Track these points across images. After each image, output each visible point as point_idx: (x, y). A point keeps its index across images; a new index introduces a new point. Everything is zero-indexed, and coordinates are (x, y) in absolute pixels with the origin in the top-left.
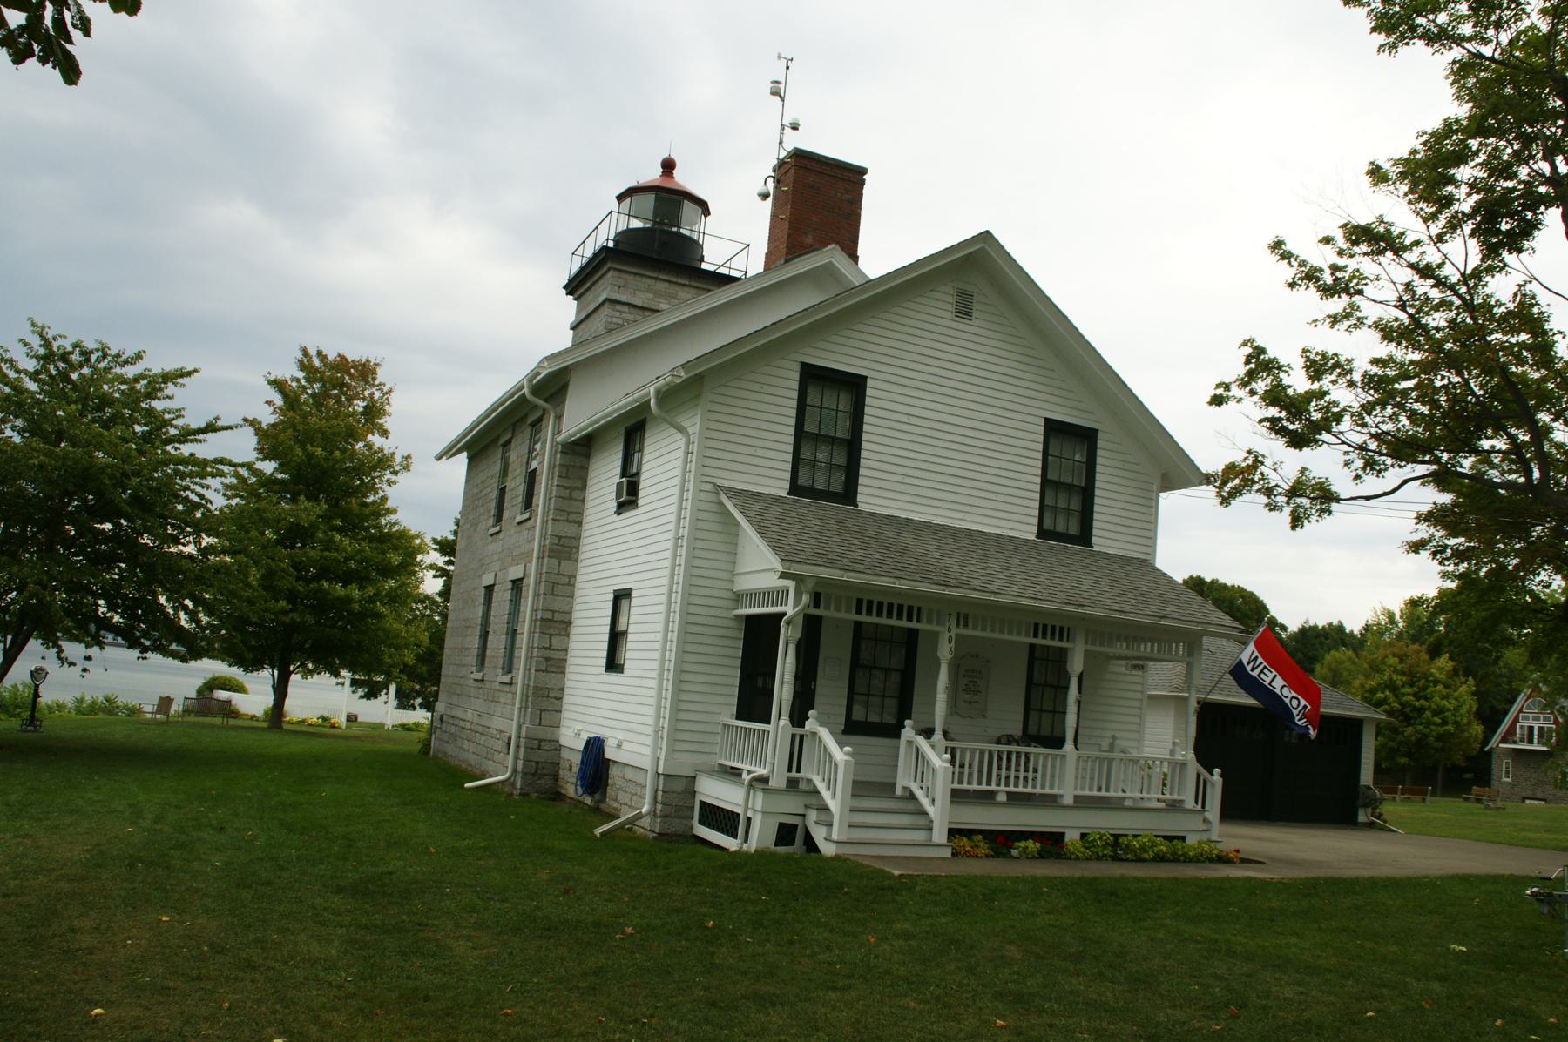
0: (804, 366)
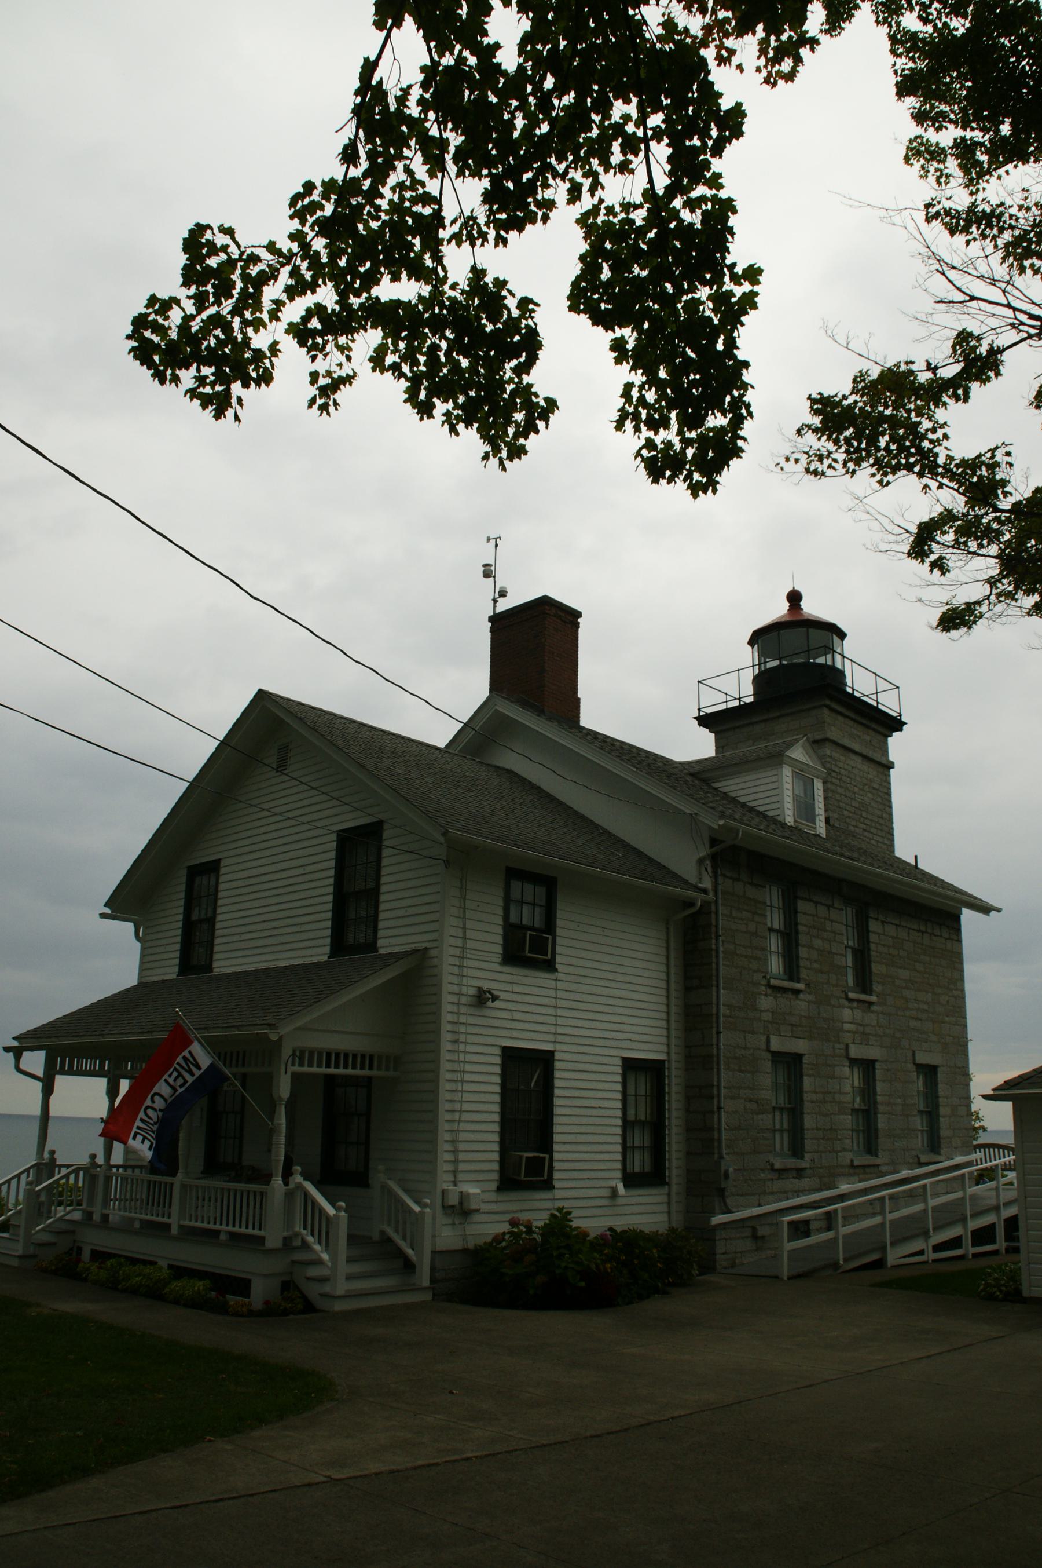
0: (189, 868)
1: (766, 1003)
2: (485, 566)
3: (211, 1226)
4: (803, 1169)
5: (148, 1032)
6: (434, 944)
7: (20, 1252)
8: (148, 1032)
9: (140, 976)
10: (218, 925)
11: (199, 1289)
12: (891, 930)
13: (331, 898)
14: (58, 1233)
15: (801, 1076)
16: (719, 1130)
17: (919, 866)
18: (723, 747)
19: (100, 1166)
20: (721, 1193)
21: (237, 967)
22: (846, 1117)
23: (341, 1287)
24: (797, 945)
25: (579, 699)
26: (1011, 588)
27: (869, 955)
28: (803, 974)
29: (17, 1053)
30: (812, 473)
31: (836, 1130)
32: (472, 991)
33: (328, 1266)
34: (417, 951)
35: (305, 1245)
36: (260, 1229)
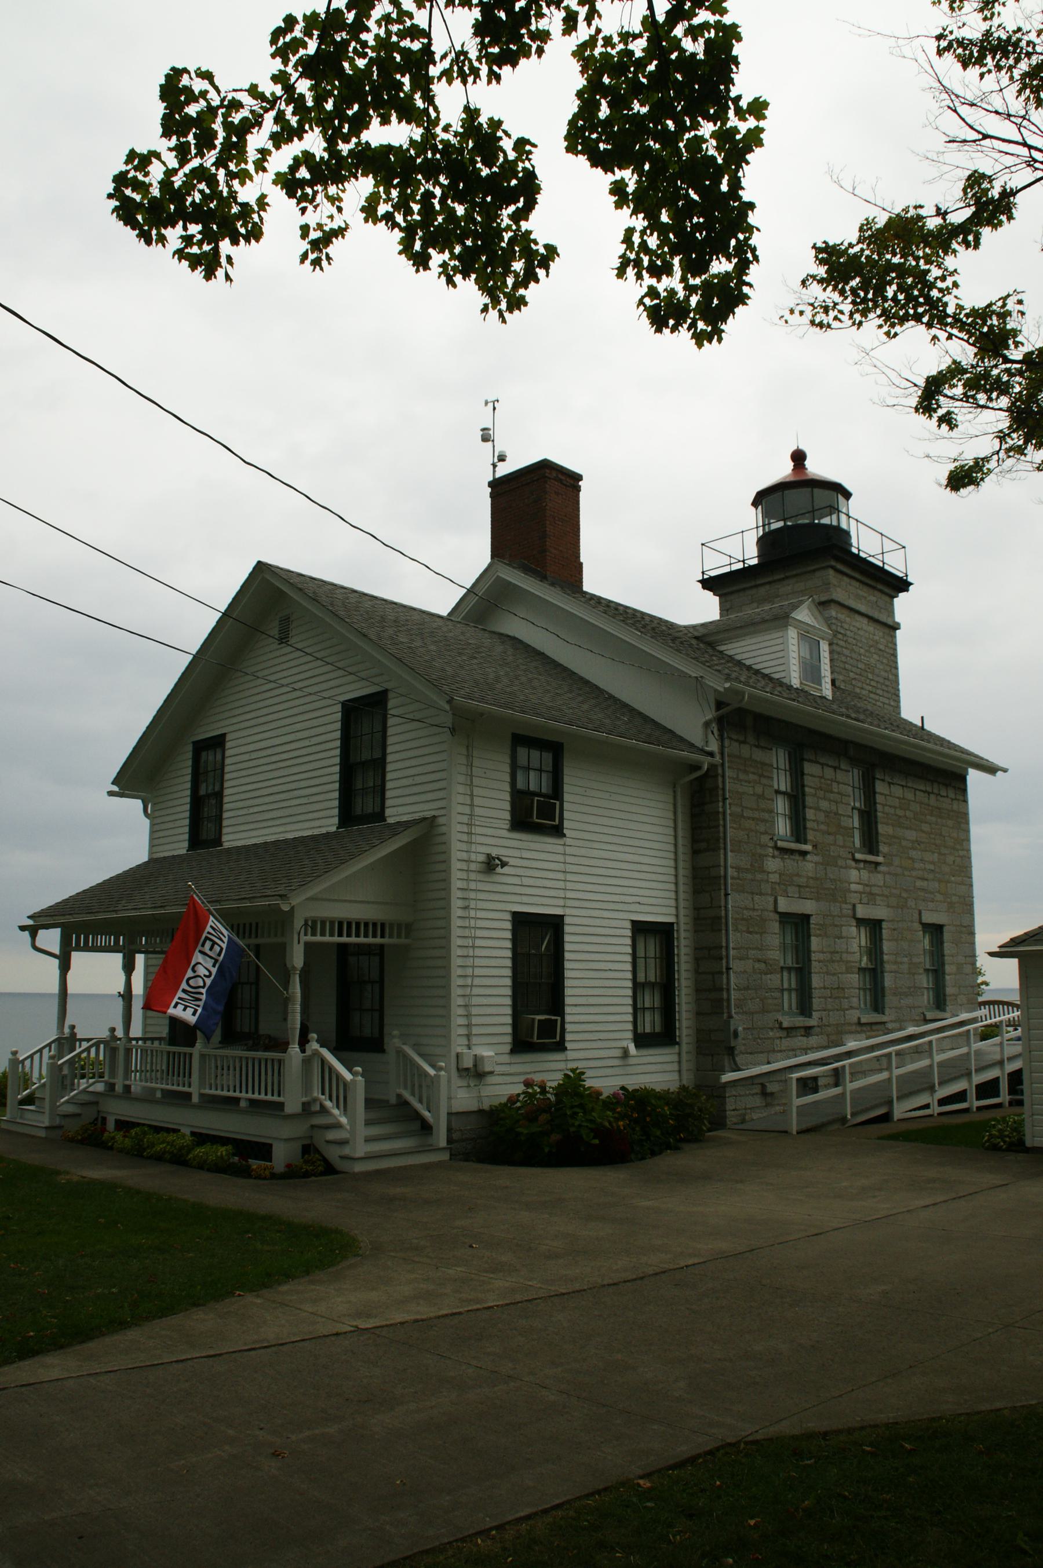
0: (195, 743)
1: (773, 864)
2: (483, 430)
3: (231, 1094)
4: (810, 1028)
5: (161, 907)
6: (442, 812)
7: (47, 1124)
8: (161, 907)
9: (151, 852)
10: (226, 800)
11: (222, 1154)
12: (898, 791)
13: (337, 769)
14: (82, 1104)
15: (809, 936)
16: (728, 990)
17: (925, 727)
18: (727, 610)
19: (120, 1039)
20: (731, 1051)
21: (247, 840)
22: (852, 976)
23: (361, 1149)
24: (804, 807)
25: (581, 564)
26: (1021, 442)
27: (876, 817)
28: (810, 835)
29: (33, 931)
30: (817, 325)
31: (843, 989)
32: (482, 858)
33: (346, 1129)
34: (425, 819)
35: (324, 1110)
36: (279, 1095)
